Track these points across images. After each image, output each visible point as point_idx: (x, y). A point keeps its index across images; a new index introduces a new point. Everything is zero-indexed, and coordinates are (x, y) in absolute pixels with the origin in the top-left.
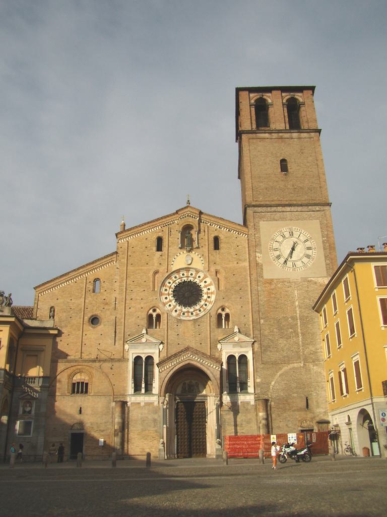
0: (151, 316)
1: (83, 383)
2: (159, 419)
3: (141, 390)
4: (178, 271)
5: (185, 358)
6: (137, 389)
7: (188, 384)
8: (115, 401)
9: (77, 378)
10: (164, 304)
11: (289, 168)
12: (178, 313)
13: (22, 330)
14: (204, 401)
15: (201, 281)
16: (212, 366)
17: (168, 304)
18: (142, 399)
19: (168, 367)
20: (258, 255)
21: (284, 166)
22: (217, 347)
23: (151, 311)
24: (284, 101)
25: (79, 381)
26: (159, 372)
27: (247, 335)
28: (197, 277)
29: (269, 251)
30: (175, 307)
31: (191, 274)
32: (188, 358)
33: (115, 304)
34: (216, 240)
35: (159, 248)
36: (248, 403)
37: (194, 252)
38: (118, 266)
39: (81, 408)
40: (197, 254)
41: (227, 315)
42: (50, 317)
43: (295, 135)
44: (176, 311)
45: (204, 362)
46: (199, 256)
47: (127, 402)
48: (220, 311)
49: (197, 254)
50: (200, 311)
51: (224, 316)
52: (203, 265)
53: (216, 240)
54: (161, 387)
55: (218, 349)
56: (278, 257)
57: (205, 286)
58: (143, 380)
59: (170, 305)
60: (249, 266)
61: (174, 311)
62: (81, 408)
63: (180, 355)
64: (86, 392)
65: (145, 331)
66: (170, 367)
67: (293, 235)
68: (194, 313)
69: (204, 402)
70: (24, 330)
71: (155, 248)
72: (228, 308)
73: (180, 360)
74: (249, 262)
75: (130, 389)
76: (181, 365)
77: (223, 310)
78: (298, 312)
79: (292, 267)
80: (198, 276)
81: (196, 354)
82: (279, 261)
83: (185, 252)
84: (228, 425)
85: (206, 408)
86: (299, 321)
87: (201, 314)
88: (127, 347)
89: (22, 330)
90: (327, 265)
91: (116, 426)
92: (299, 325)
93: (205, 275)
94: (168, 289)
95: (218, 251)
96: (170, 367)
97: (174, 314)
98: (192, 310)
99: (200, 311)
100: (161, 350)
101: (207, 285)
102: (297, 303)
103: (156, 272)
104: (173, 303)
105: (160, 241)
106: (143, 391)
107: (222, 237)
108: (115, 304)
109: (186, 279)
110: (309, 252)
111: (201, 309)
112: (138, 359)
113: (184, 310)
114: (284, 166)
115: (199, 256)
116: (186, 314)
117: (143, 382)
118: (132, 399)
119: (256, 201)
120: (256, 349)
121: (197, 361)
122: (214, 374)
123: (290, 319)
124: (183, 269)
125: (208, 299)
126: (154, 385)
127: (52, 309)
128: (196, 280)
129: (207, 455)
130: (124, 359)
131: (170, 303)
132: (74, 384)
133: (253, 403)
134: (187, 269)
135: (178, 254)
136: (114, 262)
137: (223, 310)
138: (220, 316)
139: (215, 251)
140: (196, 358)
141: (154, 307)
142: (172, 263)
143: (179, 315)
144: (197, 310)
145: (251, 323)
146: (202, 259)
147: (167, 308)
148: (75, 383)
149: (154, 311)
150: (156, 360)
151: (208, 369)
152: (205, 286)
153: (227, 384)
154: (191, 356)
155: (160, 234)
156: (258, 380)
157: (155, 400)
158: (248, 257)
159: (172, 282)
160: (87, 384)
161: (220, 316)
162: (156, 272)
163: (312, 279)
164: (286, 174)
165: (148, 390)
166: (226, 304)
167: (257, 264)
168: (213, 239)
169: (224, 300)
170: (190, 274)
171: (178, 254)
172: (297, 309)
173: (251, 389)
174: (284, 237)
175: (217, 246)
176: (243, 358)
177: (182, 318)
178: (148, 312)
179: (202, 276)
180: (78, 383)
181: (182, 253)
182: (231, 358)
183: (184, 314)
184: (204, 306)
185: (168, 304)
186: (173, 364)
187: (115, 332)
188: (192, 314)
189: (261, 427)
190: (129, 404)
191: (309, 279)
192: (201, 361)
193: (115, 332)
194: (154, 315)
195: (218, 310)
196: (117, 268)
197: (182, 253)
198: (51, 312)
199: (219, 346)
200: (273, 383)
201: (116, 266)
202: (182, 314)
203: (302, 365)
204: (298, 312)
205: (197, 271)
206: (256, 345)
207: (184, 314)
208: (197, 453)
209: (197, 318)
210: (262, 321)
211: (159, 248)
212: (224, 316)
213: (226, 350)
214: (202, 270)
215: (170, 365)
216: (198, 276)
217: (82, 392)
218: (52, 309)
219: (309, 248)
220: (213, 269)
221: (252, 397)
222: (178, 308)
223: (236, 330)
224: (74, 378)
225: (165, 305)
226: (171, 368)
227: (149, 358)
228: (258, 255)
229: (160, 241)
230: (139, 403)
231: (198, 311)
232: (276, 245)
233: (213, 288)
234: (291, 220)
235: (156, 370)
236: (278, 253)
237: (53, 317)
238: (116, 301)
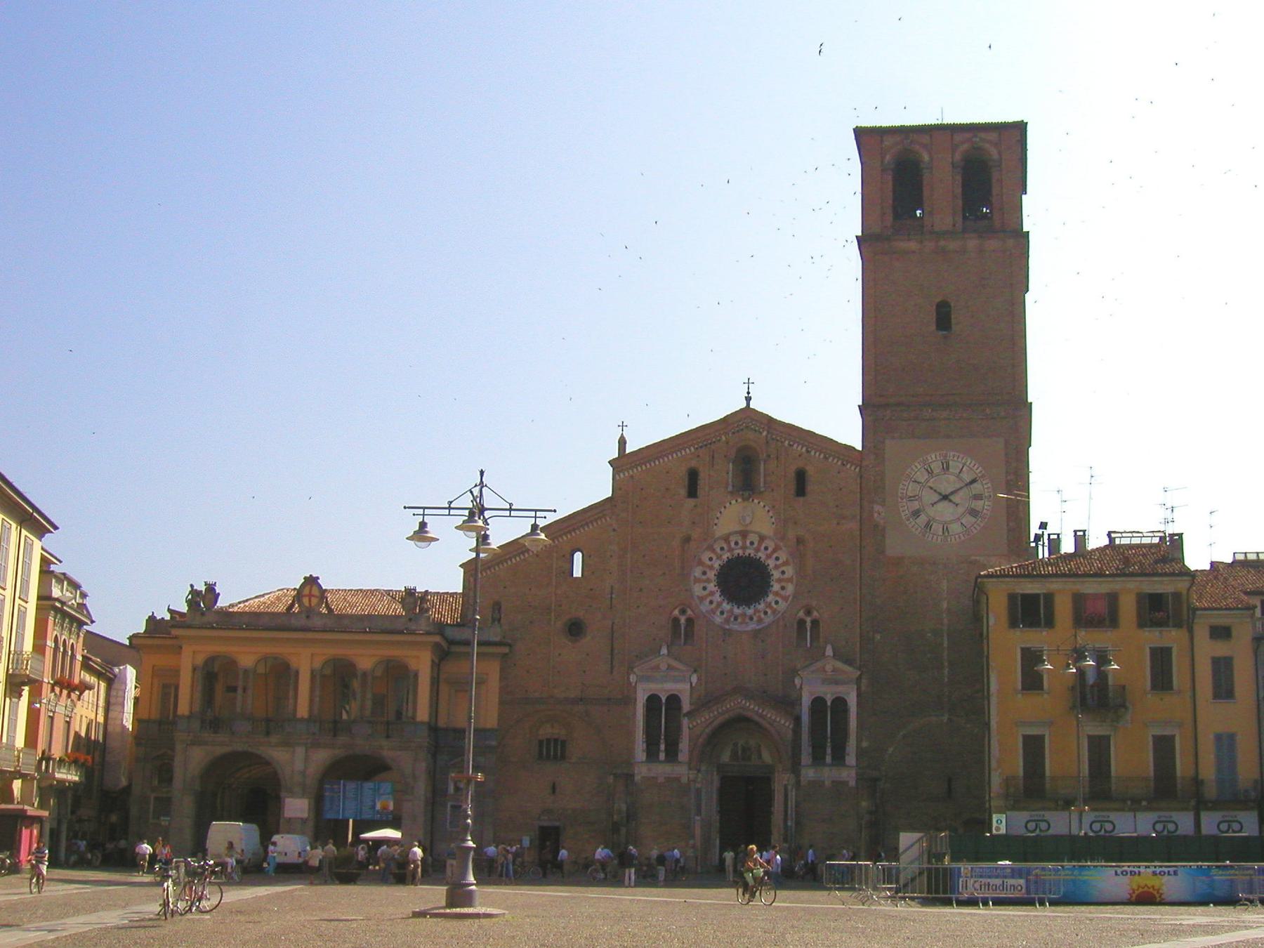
0: (676, 621)
1: (556, 740)
3: (658, 756)
4: (726, 539)
6: (652, 754)
7: (742, 745)
8: (614, 774)
9: (547, 731)
10: (702, 599)
11: (953, 321)
12: (725, 616)
13: (446, 649)
15: (769, 557)
18: (662, 770)
20: (877, 508)
21: (944, 317)
22: (794, 681)
23: (676, 612)
24: (958, 156)
25: (549, 737)
26: (689, 728)
27: (849, 662)
29: (900, 500)
30: (719, 604)
31: (752, 543)
33: (611, 598)
34: (801, 477)
35: (692, 492)
36: (845, 783)
37: (756, 501)
38: (615, 526)
39: (554, 784)
40: (762, 504)
41: (815, 623)
42: (493, 620)
43: (972, 243)
44: (722, 613)
45: (764, 713)
46: (767, 508)
47: (632, 776)
48: (801, 614)
49: (762, 504)
50: (766, 613)
51: (808, 624)
52: (774, 526)
53: (801, 477)
54: (691, 752)
55: (795, 686)
56: (916, 514)
57: (776, 567)
58: (663, 737)
59: (711, 602)
60: (861, 530)
62: (554, 784)
63: (725, 700)
64: (563, 757)
65: (664, 651)
66: (706, 720)
67: (948, 468)
68: (755, 618)
70: (448, 648)
71: (683, 492)
72: (817, 611)
74: (861, 521)
75: (640, 753)
76: (727, 716)
77: (808, 613)
78: (946, 621)
79: (941, 534)
80: (764, 545)
82: (918, 520)
83: (740, 500)
85: (773, 787)
86: (945, 638)
87: (768, 620)
88: (633, 678)
89: (446, 649)
90: (1009, 531)
91: (615, 817)
92: (945, 645)
93: (776, 545)
95: (801, 499)
96: (706, 720)
97: (718, 619)
98: (750, 612)
99: (766, 613)
100: (694, 685)
101: (782, 572)
102: (945, 605)
103: (687, 539)
104: (717, 597)
105: (693, 476)
106: (662, 756)
107: (810, 470)
108: (611, 598)
109: (740, 552)
110: (978, 505)
112: (653, 701)
113: (737, 611)
114: (944, 317)
115: (767, 508)
116: (740, 620)
117: (662, 741)
118: (642, 771)
119: (881, 396)
120: (863, 688)
121: (751, 708)
123: (929, 635)
124: (736, 532)
125: (783, 593)
126: (681, 746)
127: (497, 606)
128: (760, 554)
130: (629, 701)
132: (541, 742)
133: (852, 783)
134: (744, 534)
135: (728, 505)
136: (608, 519)
137: (808, 613)
138: (801, 623)
139: (797, 498)
140: (752, 707)
142: (716, 521)
143: (727, 621)
145: (859, 640)
146: (771, 514)
147: (705, 607)
148: (543, 741)
149: (683, 612)
150: (686, 707)
151: (771, 725)
152: (776, 567)
153: (810, 750)
155: (693, 464)
156: (865, 744)
158: (858, 512)
160: (564, 742)
161: (801, 623)
162: (687, 539)
163: (978, 558)
164: (945, 337)
165: (672, 754)
166: (814, 603)
167: (876, 526)
168: (793, 475)
171: (728, 505)
172: (944, 615)
173: (851, 759)
174: (930, 472)
175: (801, 490)
176: (840, 703)
177: (736, 627)
178: (671, 613)
179: (771, 546)
180: (548, 740)
181: (734, 502)
182: (818, 703)
183: (736, 619)
186: (711, 715)
187: (612, 650)
188: (751, 619)
189: (863, 826)
190: (637, 778)
191: (973, 558)
193: (612, 650)
194: (683, 620)
196: (614, 530)
197: (734, 502)
198: (493, 612)
199: (797, 681)
200: (891, 750)
201: (612, 525)
202: (732, 619)
203: (945, 718)
204: (946, 621)
205: (762, 538)
206: (864, 681)
207: (736, 619)
209: (760, 627)
210: (878, 637)
211: (692, 492)
212: (808, 624)
213: (810, 689)
216: (764, 545)
217: (555, 757)
218: (497, 606)
219: (977, 497)
220: (791, 534)
221: (853, 772)
222: (726, 606)
223: (829, 651)
224: (541, 732)
226: (709, 722)
227: (674, 700)
228: (877, 508)
229: (693, 476)
230: (656, 778)
231: (763, 616)
232: (912, 489)
233: (790, 571)
234: (948, 437)
235: (685, 721)
236: (916, 505)
237: (499, 620)
238: (612, 593)
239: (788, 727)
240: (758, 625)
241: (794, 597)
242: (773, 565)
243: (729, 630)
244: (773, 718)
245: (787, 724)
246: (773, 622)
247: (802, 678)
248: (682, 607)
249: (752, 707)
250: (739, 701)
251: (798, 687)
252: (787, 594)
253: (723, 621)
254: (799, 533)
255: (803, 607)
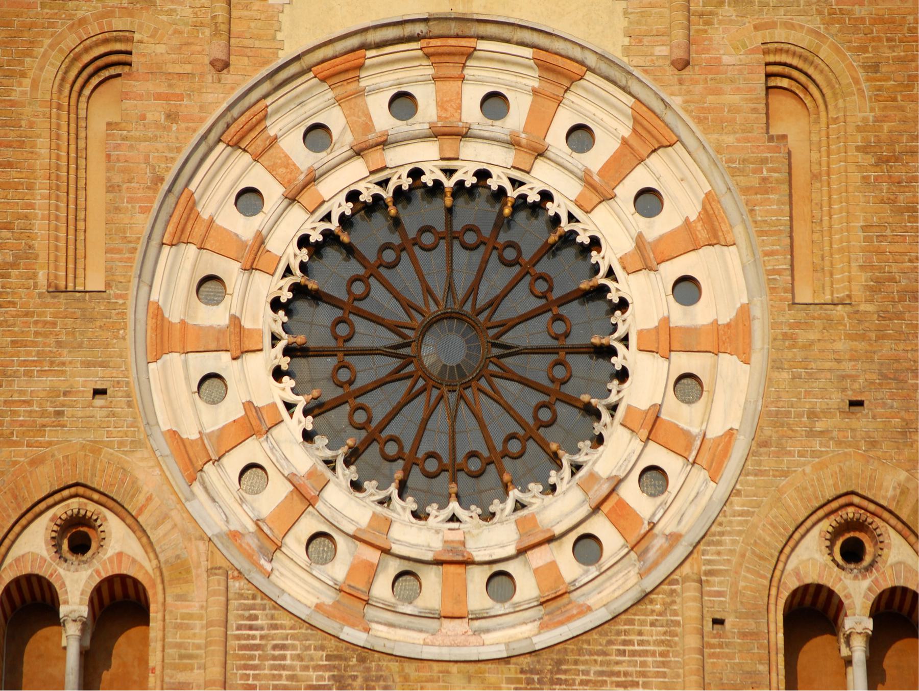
17: (235, 461)
28: (556, 138)
61: (295, 544)
80: (564, 120)
94: (230, 270)
111: (600, 527)
131: (251, 451)
141: (78, 488)
144: (551, 539)
159: (273, 192)
169: (862, 422)
170: (472, 95)
184: (631, 492)
185: (235, 461)
195: (791, 541)
202: (382, 589)
214: (615, 51)
225: (193, 473)
240: (544, 627)
241: (760, 444)
242: (627, 246)
243: (365, 653)
246: (645, 597)
248: (74, 504)
252: (716, 430)
253: (328, 597)
254: (780, 34)
255: (825, 508)
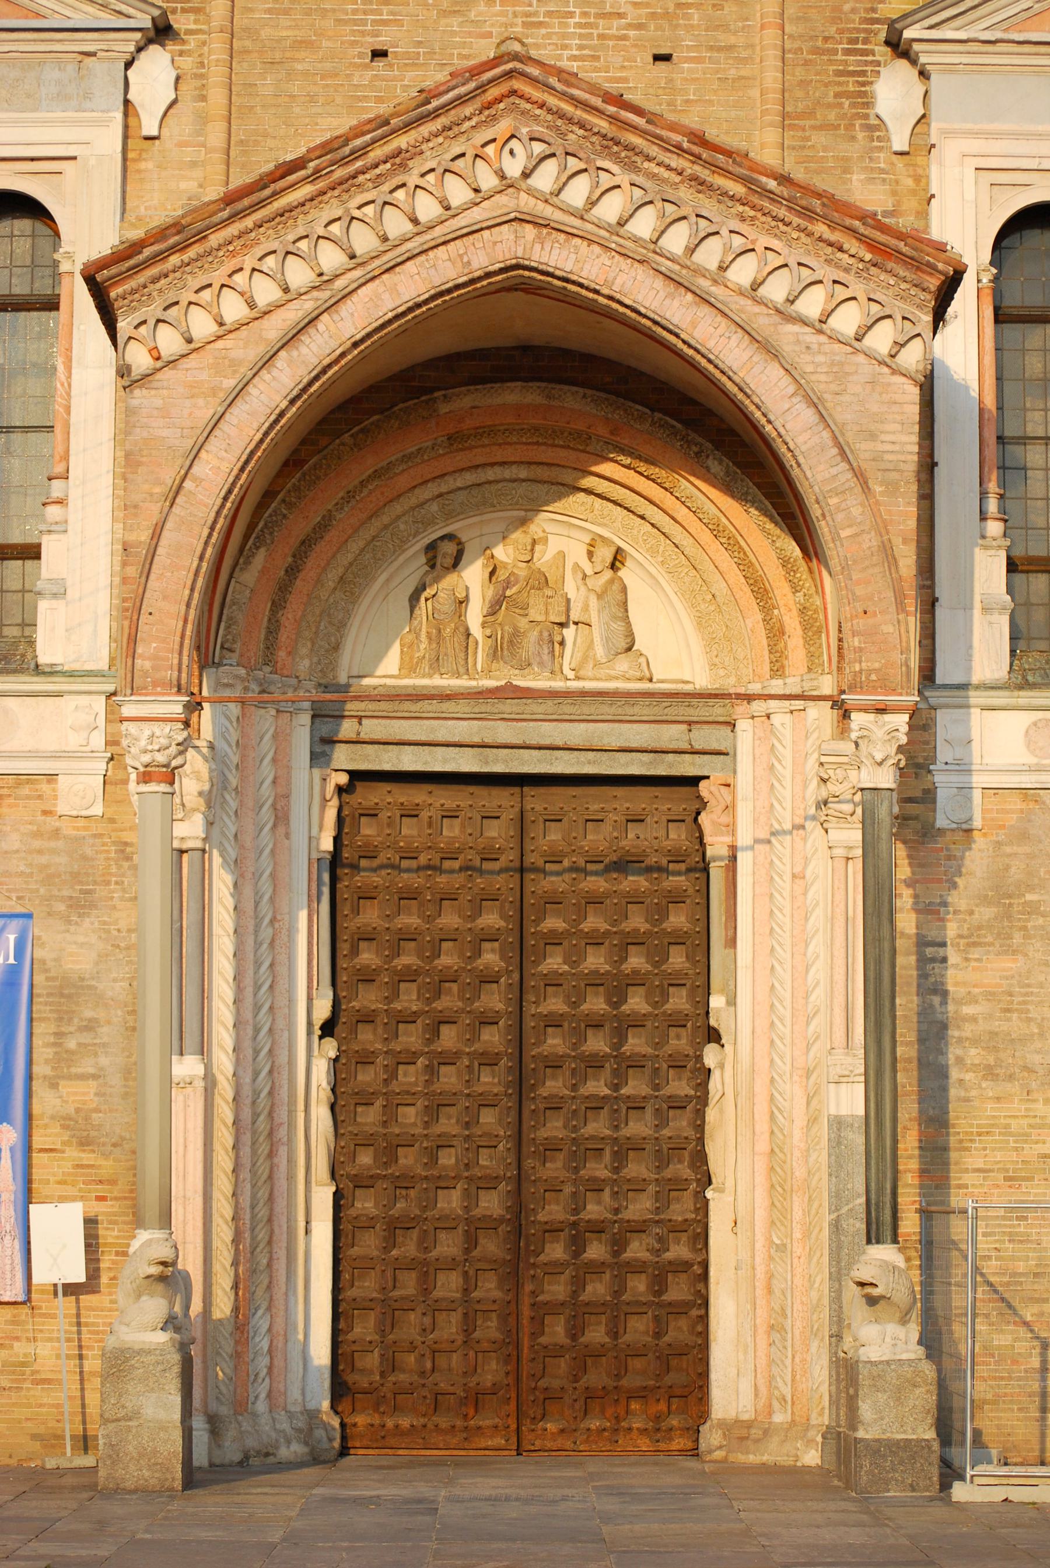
2: (113, 985)
5: (458, 192)
14: (686, 767)
16: (812, 304)
19: (233, 308)
22: (864, 99)
26: (123, 371)
32: (505, 203)
45: (709, 255)
55: (877, 128)
63: (400, 160)
69: (694, 781)
73: (396, 224)
81: (610, 144)
84: (990, 1073)
122: (843, 414)
129: (711, 1437)
140: (610, 209)
151: (769, 350)
154: (545, 178)
157: (74, 741)
186: (298, 274)
192: (676, 240)
208: (591, 1398)
215: (266, 292)
226: (275, 327)
239: (889, 362)
244: (776, 290)
245: (881, 339)
247: (924, 74)
249: (610, 209)
250: (514, 168)
251: (900, 141)
